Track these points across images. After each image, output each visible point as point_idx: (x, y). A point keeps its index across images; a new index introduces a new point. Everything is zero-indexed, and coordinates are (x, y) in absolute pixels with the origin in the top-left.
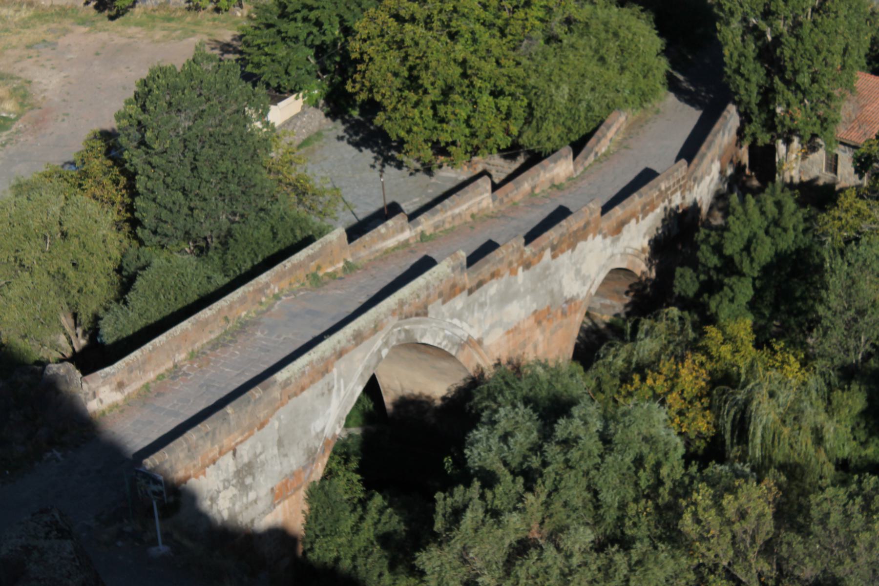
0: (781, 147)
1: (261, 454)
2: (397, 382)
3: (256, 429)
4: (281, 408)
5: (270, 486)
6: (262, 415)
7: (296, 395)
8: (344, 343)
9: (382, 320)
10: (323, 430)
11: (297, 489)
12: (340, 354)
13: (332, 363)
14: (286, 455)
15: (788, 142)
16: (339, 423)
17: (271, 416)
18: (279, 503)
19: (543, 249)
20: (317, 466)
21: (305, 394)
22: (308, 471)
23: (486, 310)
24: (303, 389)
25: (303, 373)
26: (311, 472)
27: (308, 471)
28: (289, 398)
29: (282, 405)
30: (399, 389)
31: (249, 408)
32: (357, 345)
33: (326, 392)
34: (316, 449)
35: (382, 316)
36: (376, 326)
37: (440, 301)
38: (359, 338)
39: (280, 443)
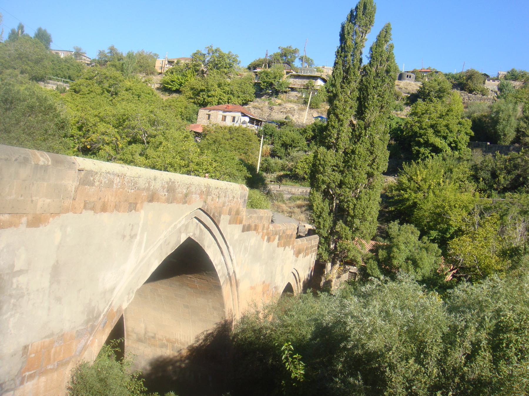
0: (329, 265)
1: (21, 272)
2: (142, 325)
3: (24, 220)
4: (70, 214)
5: (23, 341)
6: (42, 202)
7: (93, 209)
8: (157, 185)
9: (192, 193)
10: (112, 290)
11: (63, 364)
12: (152, 198)
13: (142, 202)
14: (59, 299)
15: (333, 264)
16: (129, 294)
17: (54, 214)
18: (31, 377)
19: (276, 234)
20: (93, 342)
21: (105, 216)
22: (83, 342)
23: (246, 256)
24: (104, 209)
25: (111, 182)
26: (85, 348)
27: (83, 342)
28: (85, 207)
29: (74, 210)
30: (142, 332)
31: (25, 172)
32: (169, 201)
33: (128, 238)
34: (100, 315)
35: (193, 189)
36: (186, 195)
37: (228, 217)
38: (172, 194)
39: (56, 272)
